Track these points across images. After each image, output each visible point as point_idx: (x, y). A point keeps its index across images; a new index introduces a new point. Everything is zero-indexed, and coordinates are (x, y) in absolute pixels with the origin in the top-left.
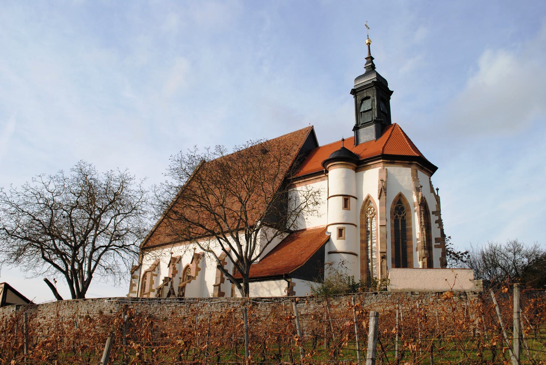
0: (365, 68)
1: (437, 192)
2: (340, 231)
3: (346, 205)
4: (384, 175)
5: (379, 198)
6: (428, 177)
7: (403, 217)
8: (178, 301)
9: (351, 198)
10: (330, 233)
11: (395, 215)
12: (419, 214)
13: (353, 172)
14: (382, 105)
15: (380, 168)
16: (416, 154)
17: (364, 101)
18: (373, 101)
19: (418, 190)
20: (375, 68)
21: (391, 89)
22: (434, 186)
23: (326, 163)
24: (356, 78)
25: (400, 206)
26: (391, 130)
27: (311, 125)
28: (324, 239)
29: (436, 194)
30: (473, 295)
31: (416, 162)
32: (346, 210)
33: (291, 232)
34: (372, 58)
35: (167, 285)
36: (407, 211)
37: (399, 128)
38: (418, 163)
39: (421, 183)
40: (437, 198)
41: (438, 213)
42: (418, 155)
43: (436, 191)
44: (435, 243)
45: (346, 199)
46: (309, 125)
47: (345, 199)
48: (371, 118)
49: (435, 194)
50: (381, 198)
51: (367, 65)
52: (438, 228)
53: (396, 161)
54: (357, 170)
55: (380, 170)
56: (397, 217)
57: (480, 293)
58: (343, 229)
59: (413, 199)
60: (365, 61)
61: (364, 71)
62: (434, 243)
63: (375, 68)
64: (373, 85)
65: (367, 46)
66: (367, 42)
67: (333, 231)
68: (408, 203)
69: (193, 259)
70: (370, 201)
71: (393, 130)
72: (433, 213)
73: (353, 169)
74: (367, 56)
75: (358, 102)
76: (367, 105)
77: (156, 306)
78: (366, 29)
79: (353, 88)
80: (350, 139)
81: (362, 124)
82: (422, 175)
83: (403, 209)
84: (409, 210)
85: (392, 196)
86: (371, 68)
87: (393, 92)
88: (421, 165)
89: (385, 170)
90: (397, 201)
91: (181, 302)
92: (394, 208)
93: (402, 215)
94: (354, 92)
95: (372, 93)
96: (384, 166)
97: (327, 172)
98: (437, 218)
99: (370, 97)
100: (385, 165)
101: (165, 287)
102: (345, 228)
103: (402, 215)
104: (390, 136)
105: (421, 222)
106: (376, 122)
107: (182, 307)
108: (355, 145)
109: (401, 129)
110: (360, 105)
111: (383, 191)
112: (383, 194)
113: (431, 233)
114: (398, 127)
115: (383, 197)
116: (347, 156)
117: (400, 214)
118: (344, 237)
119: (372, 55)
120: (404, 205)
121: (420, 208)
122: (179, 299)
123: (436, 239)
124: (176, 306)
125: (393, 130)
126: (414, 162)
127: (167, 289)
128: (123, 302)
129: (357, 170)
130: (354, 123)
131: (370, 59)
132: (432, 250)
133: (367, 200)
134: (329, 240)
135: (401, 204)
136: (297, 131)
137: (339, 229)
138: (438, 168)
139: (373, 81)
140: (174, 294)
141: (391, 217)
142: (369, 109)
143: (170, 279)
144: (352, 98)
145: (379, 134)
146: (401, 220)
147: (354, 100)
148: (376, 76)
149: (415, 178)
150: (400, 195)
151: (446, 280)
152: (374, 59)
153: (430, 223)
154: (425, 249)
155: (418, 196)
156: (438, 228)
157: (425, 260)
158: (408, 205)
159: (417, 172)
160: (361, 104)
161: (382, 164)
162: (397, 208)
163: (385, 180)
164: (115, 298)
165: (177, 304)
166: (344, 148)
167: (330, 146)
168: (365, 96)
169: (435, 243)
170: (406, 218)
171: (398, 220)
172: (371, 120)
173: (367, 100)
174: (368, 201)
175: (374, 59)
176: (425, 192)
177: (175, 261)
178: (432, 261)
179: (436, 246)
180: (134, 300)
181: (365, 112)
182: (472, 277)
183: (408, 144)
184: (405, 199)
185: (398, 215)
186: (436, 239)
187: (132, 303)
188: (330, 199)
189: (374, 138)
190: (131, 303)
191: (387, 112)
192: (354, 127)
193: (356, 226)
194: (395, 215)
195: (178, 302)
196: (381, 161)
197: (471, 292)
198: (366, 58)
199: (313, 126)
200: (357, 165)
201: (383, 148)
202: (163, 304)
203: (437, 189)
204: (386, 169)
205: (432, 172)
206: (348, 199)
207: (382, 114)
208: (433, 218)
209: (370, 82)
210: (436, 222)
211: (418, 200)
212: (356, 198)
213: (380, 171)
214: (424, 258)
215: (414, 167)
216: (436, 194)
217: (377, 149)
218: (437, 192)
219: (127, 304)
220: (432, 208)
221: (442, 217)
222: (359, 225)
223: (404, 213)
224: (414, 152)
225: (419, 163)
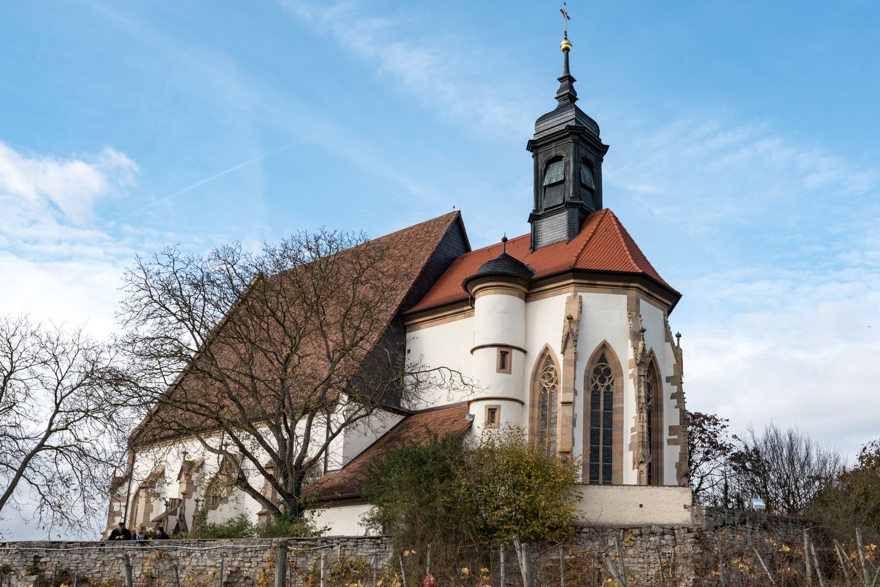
0: (556, 98)
1: (678, 340)
2: (492, 413)
3: (503, 365)
4: (575, 308)
5: (563, 353)
6: (660, 313)
7: (608, 387)
8: (138, 546)
9: (514, 352)
10: (473, 416)
11: (592, 383)
12: (637, 381)
13: (520, 302)
15: (570, 294)
16: (637, 268)
17: (551, 165)
18: (567, 164)
20: (577, 99)
21: (604, 142)
22: (671, 330)
23: (468, 283)
24: (537, 119)
25: (603, 366)
26: (597, 223)
27: (456, 209)
28: (457, 427)
29: (676, 345)
30: (686, 535)
31: (637, 285)
32: (503, 372)
33: (409, 414)
34: (572, 80)
35: (174, 513)
36: (616, 377)
37: (613, 219)
38: (640, 287)
39: (645, 325)
40: (678, 353)
41: (677, 379)
42: (640, 271)
43: (675, 339)
44: (670, 435)
45: (505, 352)
46: (454, 210)
47: (501, 352)
48: (562, 198)
49: (673, 344)
50: (567, 352)
51: (561, 94)
52: (676, 407)
53: (598, 283)
54: (527, 298)
55: (569, 298)
56: (596, 387)
57: (700, 531)
58: (496, 409)
60: (559, 85)
61: (554, 105)
62: (666, 436)
63: (577, 99)
64: (567, 133)
65: (563, 55)
66: (563, 46)
67: (478, 411)
68: (619, 362)
69: (182, 471)
70: (549, 357)
71: (600, 222)
72: (668, 379)
73: (520, 297)
74: (562, 74)
75: (540, 167)
76: (556, 173)
77: (94, 556)
78: (564, 19)
79: (532, 138)
80: (523, 238)
81: (546, 210)
83: (608, 371)
84: (621, 374)
85: (589, 347)
86: (568, 97)
87: (608, 146)
88: (647, 290)
89: (577, 298)
90: (598, 358)
91: (143, 549)
92: (592, 371)
93: (606, 384)
94: (533, 146)
95: (567, 150)
96: (575, 292)
97: (472, 300)
98: (675, 389)
99: (563, 157)
100: (577, 289)
101: (171, 518)
102: (499, 406)
103: (606, 384)
104: (594, 234)
105: (639, 397)
107: (147, 558)
108: (531, 250)
109: (616, 219)
110: (543, 173)
111: (571, 338)
112: (570, 344)
113: (662, 416)
114: (611, 215)
115: (570, 350)
116: (509, 271)
117: (602, 380)
118: (499, 424)
119: (572, 74)
120: (610, 365)
121: (639, 370)
122: (140, 542)
123: (671, 428)
124: (135, 555)
125: (600, 222)
126: (632, 285)
127: (173, 521)
128: (29, 551)
129: (527, 298)
130: (530, 207)
131: (568, 79)
132: (662, 448)
133: (543, 355)
134: (470, 427)
135: (606, 362)
136: (431, 221)
137: (489, 409)
138: (681, 296)
139: (567, 126)
140: (185, 530)
141: (586, 388)
142: (558, 180)
143: (180, 501)
144: (528, 158)
145: (574, 230)
146: (605, 393)
147: (532, 161)
148: (574, 116)
149: (634, 312)
150: (604, 346)
151: (641, 506)
152: (575, 81)
153: (662, 399)
154: (643, 447)
156: (676, 407)
157: (644, 467)
158: (618, 364)
159: (638, 302)
160: (546, 170)
162: (597, 371)
163: (575, 317)
164: (14, 543)
165: (137, 552)
166: (506, 257)
167: (489, 249)
168: (553, 154)
169: (670, 435)
170: (613, 389)
171: (599, 392)
172: (561, 202)
173: (557, 163)
174: (546, 357)
175: (575, 81)
176: (653, 340)
177: (189, 468)
178: (662, 469)
179: (670, 442)
180: (51, 547)
181: (551, 185)
182: (689, 502)
183: (625, 248)
184: (613, 354)
185: (599, 384)
186: (671, 428)
187: (46, 551)
188: (475, 352)
190: (44, 553)
191: (594, 187)
192: (531, 215)
193: (523, 403)
194: (592, 383)
195: (137, 549)
196: (572, 281)
197: (684, 528)
198: (559, 79)
199: (460, 211)
200: (529, 289)
201: (578, 257)
202: (108, 553)
203: (679, 336)
204: (581, 297)
205: (670, 303)
206: (507, 353)
207: (583, 190)
208: (668, 389)
209: (563, 127)
210: (673, 397)
211: (636, 355)
212: (525, 352)
214: (642, 462)
215: (633, 293)
216: (676, 345)
217: (565, 259)
218: (678, 340)
219: (37, 554)
220: (666, 369)
221: (685, 388)
222: (527, 402)
223: (610, 379)
224: (634, 265)
225: (644, 285)
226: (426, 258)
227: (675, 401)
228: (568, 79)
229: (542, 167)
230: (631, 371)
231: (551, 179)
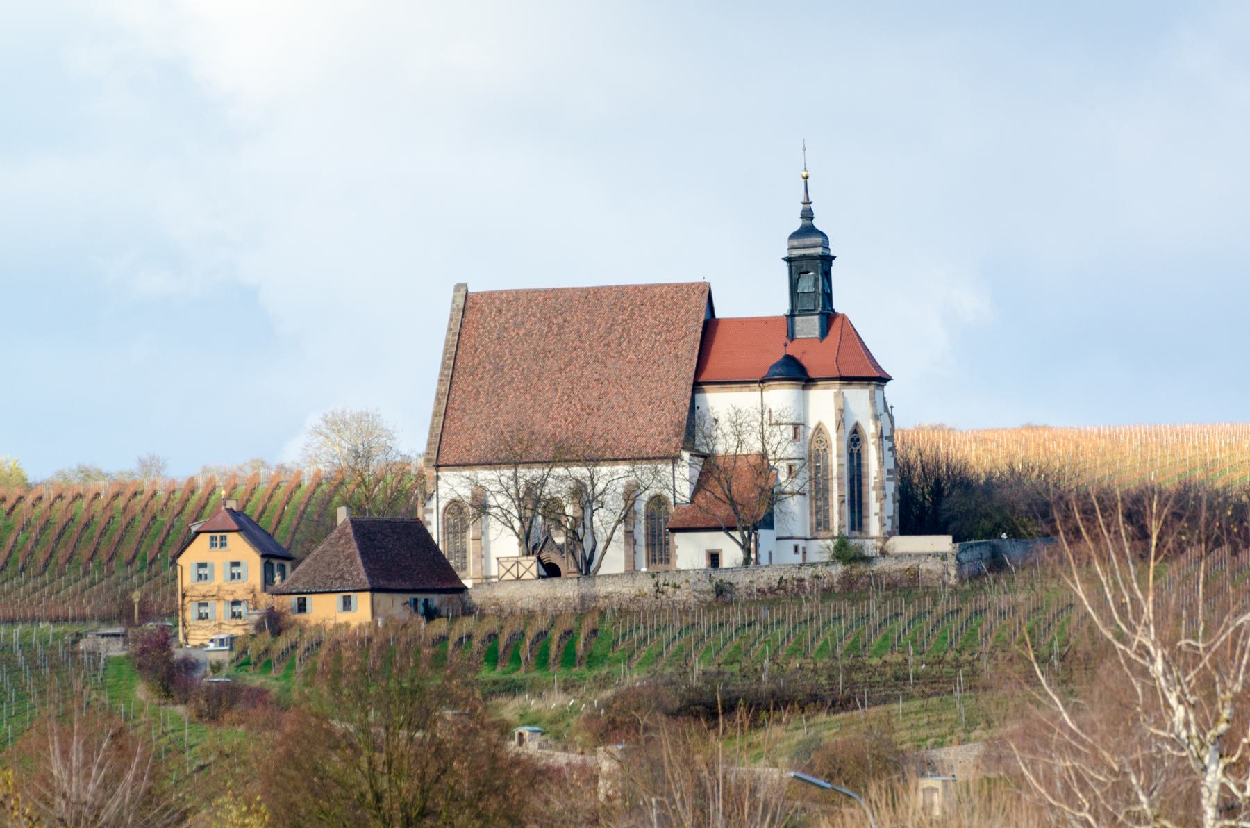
4: (841, 400)
14: (826, 284)
18: (816, 280)
19: (876, 417)
45: (796, 426)
59: (870, 429)
60: (800, 207)
72: (887, 438)
82: (878, 392)
83: (858, 440)
85: (849, 427)
86: (808, 215)
94: (789, 260)
98: (890, 444)
106: (821, 314)
111: (841, 422)
131: (807, 202)
133: (817, 428)
145: (825, 330)
150: (857, 424)
155: (877, 427)
161: (838, 387)
162: (852, 440)
174: (819, 429)
189: (817, 334)
210: (890, 449)
213: (836, 395)
226: (700, 330)
227: (891, 453)
228: (807, 202)
229: (795, 276)
230: (873, 440)
231: (803, 288)
